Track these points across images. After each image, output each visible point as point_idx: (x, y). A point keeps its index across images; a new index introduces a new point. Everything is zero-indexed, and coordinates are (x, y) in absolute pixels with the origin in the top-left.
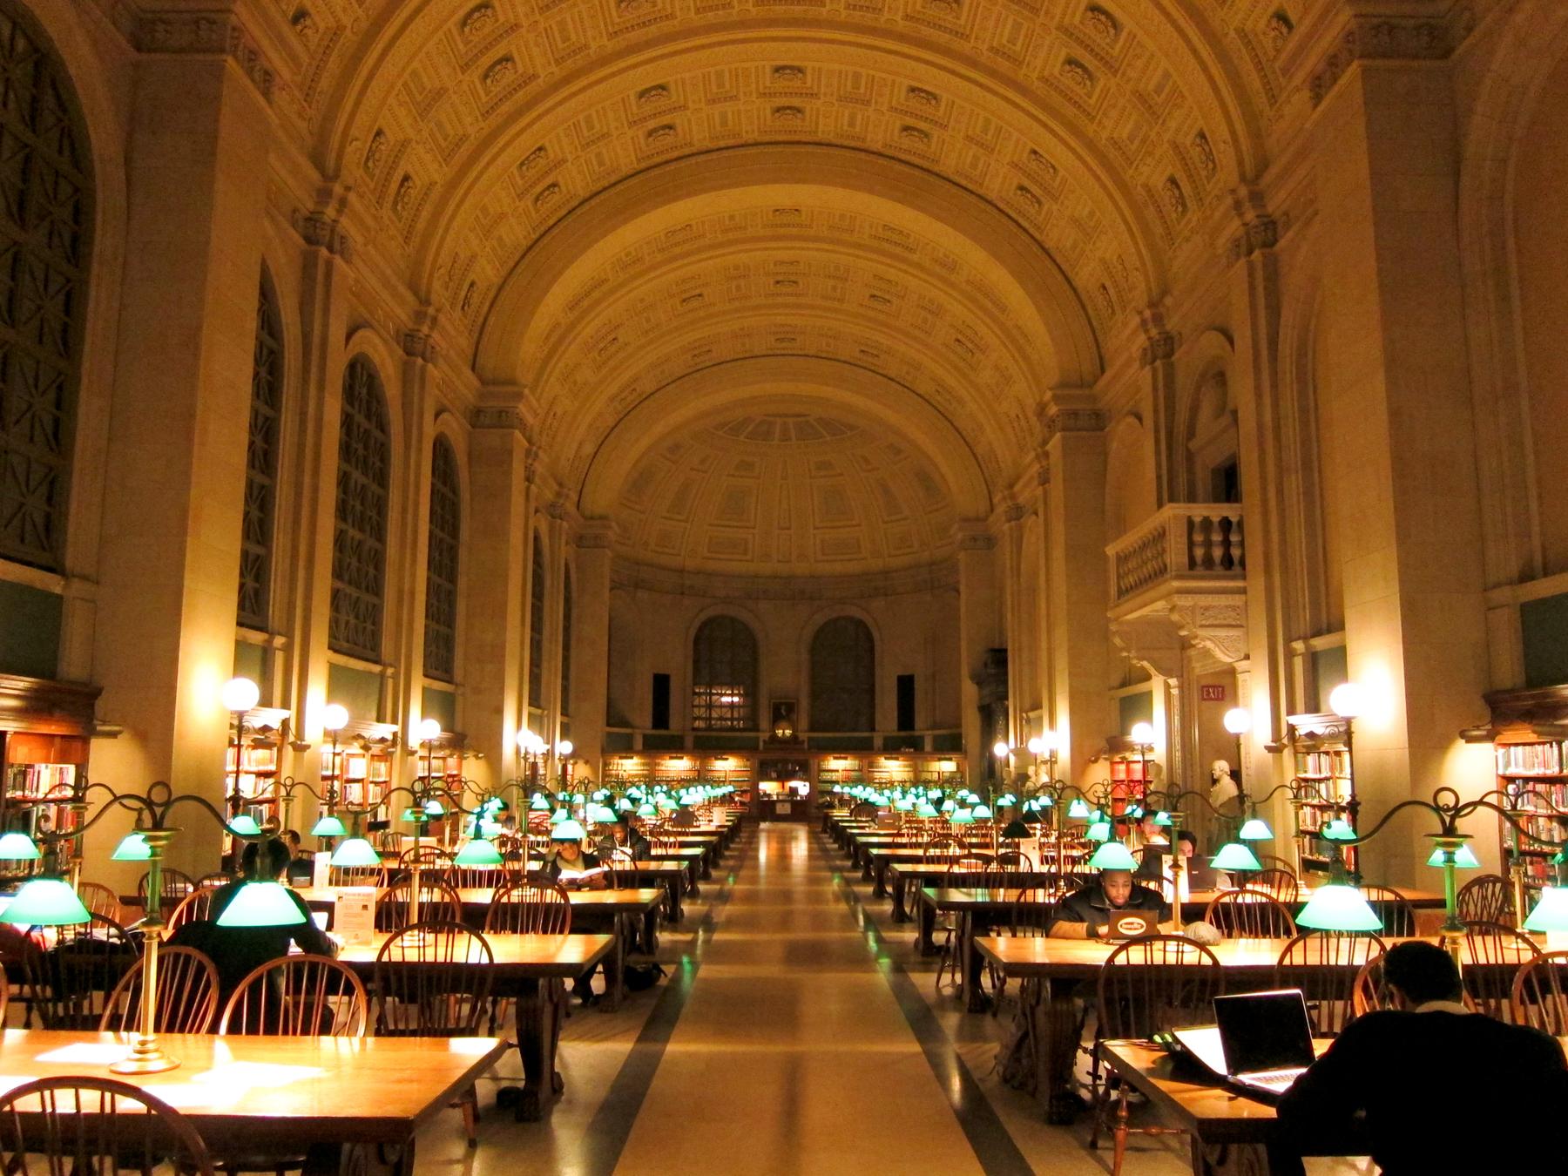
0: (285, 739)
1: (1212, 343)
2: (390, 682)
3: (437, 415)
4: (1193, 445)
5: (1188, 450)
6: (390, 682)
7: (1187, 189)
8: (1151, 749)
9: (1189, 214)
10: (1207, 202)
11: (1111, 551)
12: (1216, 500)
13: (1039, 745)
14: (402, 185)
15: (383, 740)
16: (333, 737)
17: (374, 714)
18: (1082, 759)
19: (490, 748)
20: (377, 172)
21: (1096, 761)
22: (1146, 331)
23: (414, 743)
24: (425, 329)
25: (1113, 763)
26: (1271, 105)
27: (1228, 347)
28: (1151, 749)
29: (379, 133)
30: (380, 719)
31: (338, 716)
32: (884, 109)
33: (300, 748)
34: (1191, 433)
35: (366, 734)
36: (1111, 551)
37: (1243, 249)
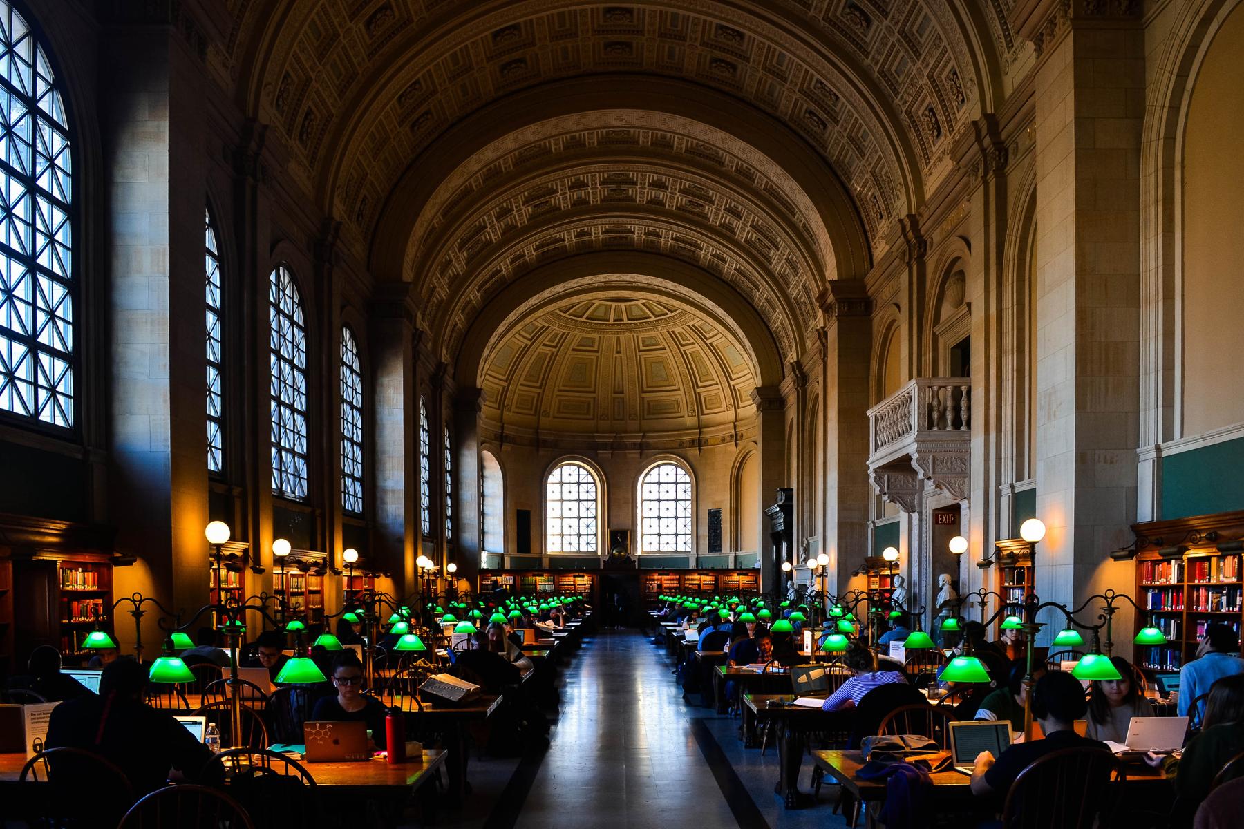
0: (249, 561)
1: (957, 246)
2: (319, 520)
3: (343, 308)
4: (938, 330)
5: (934, 333)
6: (319, 520)
7: (941, 118)
8: (897, 566)
9: (942, 139)
10: (956, 129)
11: (869, 413)
12: (953, 375)
13: (811, 564)
14: (306, 118)
15: (316, 564)
16: (280, 561)
17: (308, 545)
18: (845, 573)
19: (395, 570)
20: (286, 108)
21: (856, 575)
22: (906, 236)
23: (339, 564)
24: (330, 238)
25: (869, 577)
26: (1009, 49)
27: (967, 250)
28: (897, 566)
29: (287, 75)
30: (314, 549)
31: (282, 547)
32: (698, 44)
33: (258, 570)
34: (937, 320)
35: (304, 559)
36: (869, 413)
37: (981, 172)
